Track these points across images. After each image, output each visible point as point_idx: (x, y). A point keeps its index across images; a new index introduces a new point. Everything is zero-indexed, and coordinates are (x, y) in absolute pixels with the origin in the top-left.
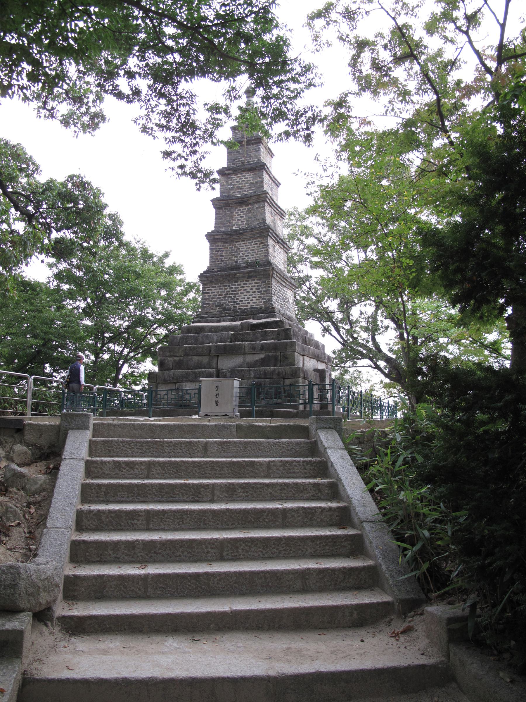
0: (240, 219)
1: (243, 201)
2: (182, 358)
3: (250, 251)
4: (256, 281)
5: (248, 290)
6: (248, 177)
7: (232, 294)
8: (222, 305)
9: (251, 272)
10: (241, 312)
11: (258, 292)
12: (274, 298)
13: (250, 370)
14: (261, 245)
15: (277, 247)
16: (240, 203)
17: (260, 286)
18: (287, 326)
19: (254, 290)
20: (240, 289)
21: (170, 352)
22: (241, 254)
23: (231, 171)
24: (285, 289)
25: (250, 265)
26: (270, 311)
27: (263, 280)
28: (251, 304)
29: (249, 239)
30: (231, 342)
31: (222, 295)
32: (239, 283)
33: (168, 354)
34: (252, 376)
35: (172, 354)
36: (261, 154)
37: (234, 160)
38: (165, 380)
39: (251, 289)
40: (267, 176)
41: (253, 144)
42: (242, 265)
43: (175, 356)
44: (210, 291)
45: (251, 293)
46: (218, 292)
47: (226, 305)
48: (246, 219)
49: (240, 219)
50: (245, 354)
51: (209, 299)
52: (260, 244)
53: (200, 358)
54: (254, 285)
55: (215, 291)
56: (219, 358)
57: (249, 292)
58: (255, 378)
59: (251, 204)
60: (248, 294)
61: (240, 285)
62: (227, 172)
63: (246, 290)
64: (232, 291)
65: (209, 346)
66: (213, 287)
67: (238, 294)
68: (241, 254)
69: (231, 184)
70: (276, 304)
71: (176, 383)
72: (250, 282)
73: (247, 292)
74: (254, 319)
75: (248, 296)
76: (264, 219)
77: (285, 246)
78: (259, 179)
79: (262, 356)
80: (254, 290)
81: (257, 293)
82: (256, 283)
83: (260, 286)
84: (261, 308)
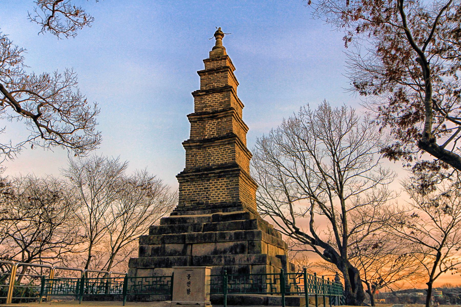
0: (211, 129)
1: (214, 115)
3: (220, 156)
4: (225, 180)
6: (218, 97)
7: (205, 191)
8: (197, 200)
9: (221, 172)
12: (241, 194)
14: (229, 151)
15: (242, 153)
18: (252, 218)
19: (224, 187)
20: (211, 186)
22: (212, 158)
23: (204, 93)
24: (249, 188)
25: (220, 167)
26: (238, 205)
27: (231, 179)
28: (221, 199)
29: (219, 146)
30: (203, 232)
32: (211, 181)
34: (223, 262)
36: (228, 80)
37: (207, 85)
39: (221, 187)
40: (233, 97)
41: (222, 72)
42: (213, 167)
44: (187, 189)
45: (221, 190)
46: (192, 190)
47: (199, 200)
48: (216, 130)
49: (211, 129)
51: (185, 195)
52: (228, 150)
54: (223, 183)
55: (191, 188)
56: (194, 246)
57: (219, 189)
59: (220, 118)
60: (218, 191)
61: (212, 183)
62: (201, 94)
63: (216, 187)
64: (205, 188)
65: (185, 235)
66: (188, 185)
67: (210, 190)
68: (212, 158)
69: (203, 104)
70: (242, 199)
74: (223, 212)
75: (218, 191)
76: (231, 130)
77: (248, 153)
78: (226, 99)
79: (231, 244)
81: (226, 190)
82: (225, 182)
83: (229, 184)
84: (230, 202)
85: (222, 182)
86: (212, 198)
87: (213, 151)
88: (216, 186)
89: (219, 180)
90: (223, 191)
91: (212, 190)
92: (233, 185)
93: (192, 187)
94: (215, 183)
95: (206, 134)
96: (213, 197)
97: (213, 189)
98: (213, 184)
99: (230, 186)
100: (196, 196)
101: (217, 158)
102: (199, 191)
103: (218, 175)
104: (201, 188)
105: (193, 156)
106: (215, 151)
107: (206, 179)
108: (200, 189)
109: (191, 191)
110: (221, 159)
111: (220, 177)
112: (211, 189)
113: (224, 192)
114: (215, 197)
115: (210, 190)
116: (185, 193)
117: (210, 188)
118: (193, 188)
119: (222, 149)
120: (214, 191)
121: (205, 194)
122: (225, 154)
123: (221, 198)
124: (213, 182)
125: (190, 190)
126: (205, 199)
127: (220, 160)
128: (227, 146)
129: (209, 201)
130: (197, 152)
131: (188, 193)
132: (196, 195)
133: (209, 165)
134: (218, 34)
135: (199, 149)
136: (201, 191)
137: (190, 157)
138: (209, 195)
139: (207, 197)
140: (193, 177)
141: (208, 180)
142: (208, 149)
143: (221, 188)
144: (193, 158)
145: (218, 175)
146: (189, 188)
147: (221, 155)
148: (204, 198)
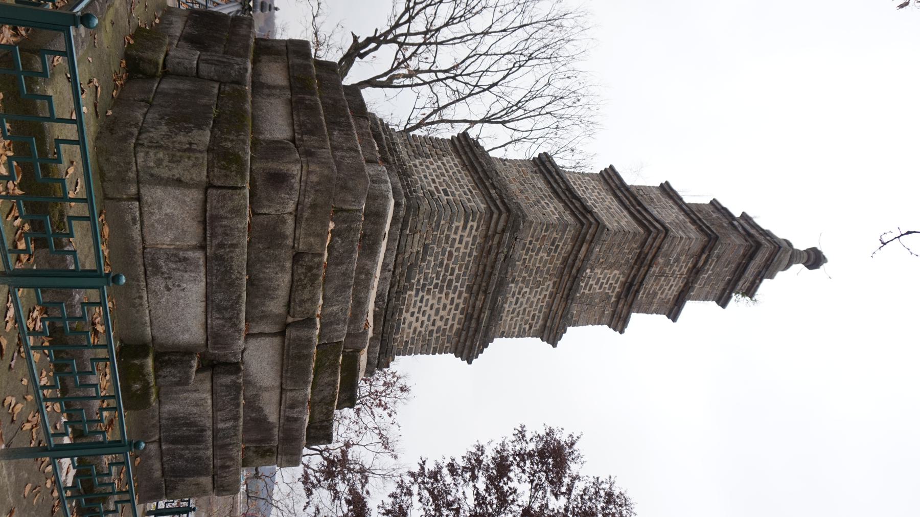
2: (289, 242)
5: (442, 313)
7: (443, 281)
8: (423, 260)
10: (395, 307)
11: (431, 332)
13: (236, 419)
16: (631, 285)
17: (443, 335)
20: (451, 296)
21: (313, 206)
22: (525, 290)
28: (409, 319)
29: (550, 306)
32: (464, 295)
33: (308, 201)
34: (221, 425)
35: (306, 214)
38: (216, 218)
39: (442, 318)
43: (297, 220)
44: (466, 234)
46: (458, 249)
50: (282, 390)
53: (282, 293)
56: (277, 341)
58: (215, 431)
59: (618, 302)
60: (433, 312)
63: (445, 307)
64: (451, 281)
67: (441, 292)
69: (677, 260)
71: (203, 247)
72: (458, 316)
73: (438, 310)
79: (273, 418)
80: (439, 323)
81: (431, 328)
86: (419, 298)
88: (449, 307)
91: (440, 298)
93: (466, 248)
94: (457, 305)
95: (596, 271)
96: (421, 301)
97: (443, 301)
98: (456, 301)
102: (447, 265)
103: (475, 316)
105: (553, 244)
106: (541, 297)
107: (475, 287)
109: (457, 245)
110: (514, 309)
111: (468, 317)
112: (443, 295)
114: (419, 304)
116: (457, 228)
117: (447, 294)
118: (462, 250)
119: (540, 312)
120: (435, 302)
121: (435, 281)
122: (522, 319)
123: (413, 319)
124: (461, 301)
126: (422, 282)
127: (513, 306)
128: (541, 322)
129: (413, 293)
131: (453, 236)
133: (512, 282)
134: (814, 259)
135: (565, 260)
136: (446, 271)
137: (554, 235)
138: (429, 290)
139: (424, 285)
140: (493, 255)
141: (470, 289)
142: (555, 283)
143: (438, 318)
144: (547, 244)
145: (475, 316)
146: (465, 239)
147: (525, 309)
148: (426, 279)
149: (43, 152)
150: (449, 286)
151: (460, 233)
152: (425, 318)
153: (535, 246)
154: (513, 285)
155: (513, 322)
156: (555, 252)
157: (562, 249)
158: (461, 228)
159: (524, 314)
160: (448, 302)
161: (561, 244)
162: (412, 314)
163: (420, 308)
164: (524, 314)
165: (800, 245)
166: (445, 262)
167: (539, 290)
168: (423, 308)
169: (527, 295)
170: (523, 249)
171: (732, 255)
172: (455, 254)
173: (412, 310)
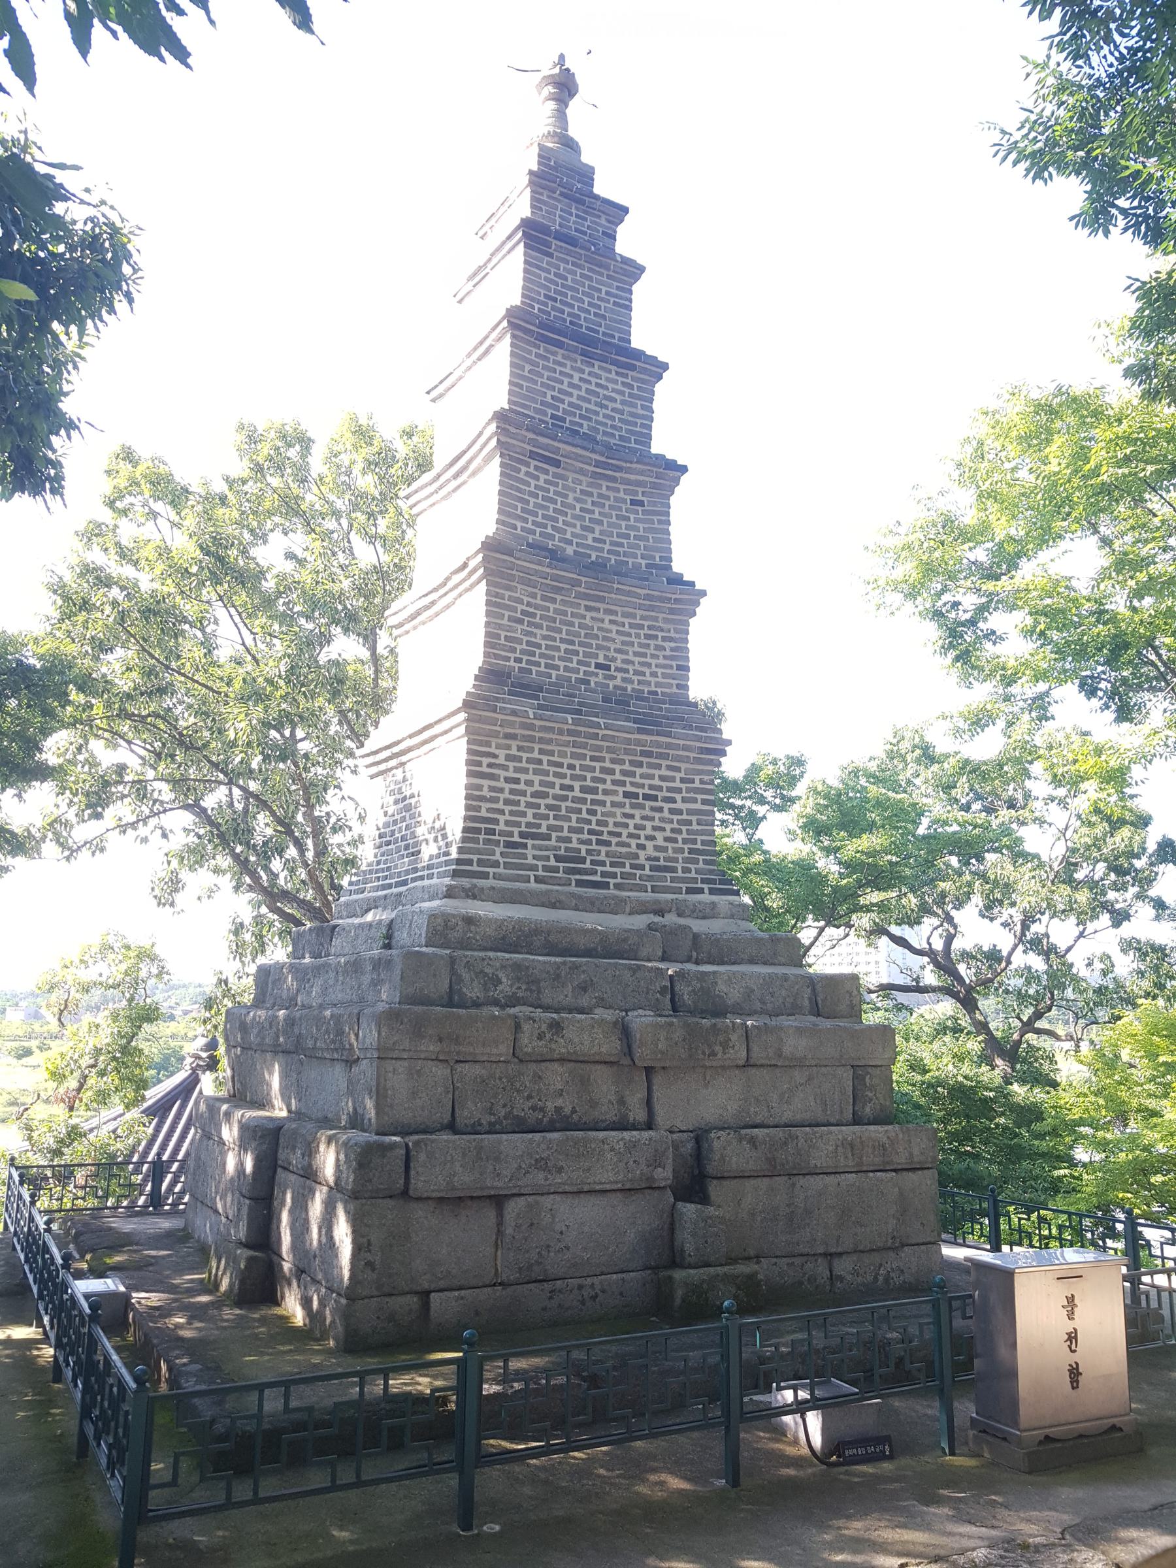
20: (609, 786)
31: (545, 795)
44: (503, 774)
46: (529, 783)
61: (612, 772)
64: (583, 789)
85: (652, 777)
86: (614, 840)
87: (606, 625)
89: (640, 765)
90: (657, 815)
91: (613, 804)
92: (695, 801)
93: (526, 771)
94: (624, 773)
99: (684, 800)
100: (547, 817)
101: (619, 664)
102: (555, 797)
104: (567, 782)
106: (614, 628)
108: (563, 787)
109: (522, 786)
113: (657, 823)
114: (624, 838)
115: (603, 803)
116: (492, 789)
118: (530, 777)
119: (641, 627)
121: (584, 815)
122: (653, 656)
123: (650, 845)
125: (517, 781)
127: (630, 675)
130: (537, 607)
131: (506, 795)
132: (543, 810)
136: (565, 798)
138: (599, 823)
146: (511, 774)
149: (301, 1426)
150: (594, 791)
151: (501, 784)
152: (649, 824)
153: (523, 652)
154: (593, 680)
155: (660, 671)
156: (534, 615)
157: (529, 604)
158: (493, 783)
159: (644, 655)
160: (621, 789)
161: (520, 607)
162: (642, 847)
163: (630, 835)
164: (644, 655)
165: (538, 117)
166: (550, 801)
167: (600, 634)
168: (631, 830)
169: (612, 654)
170: (530, 672)
171: (571, 225)
172: (537, 787)
173: (634, 849)
